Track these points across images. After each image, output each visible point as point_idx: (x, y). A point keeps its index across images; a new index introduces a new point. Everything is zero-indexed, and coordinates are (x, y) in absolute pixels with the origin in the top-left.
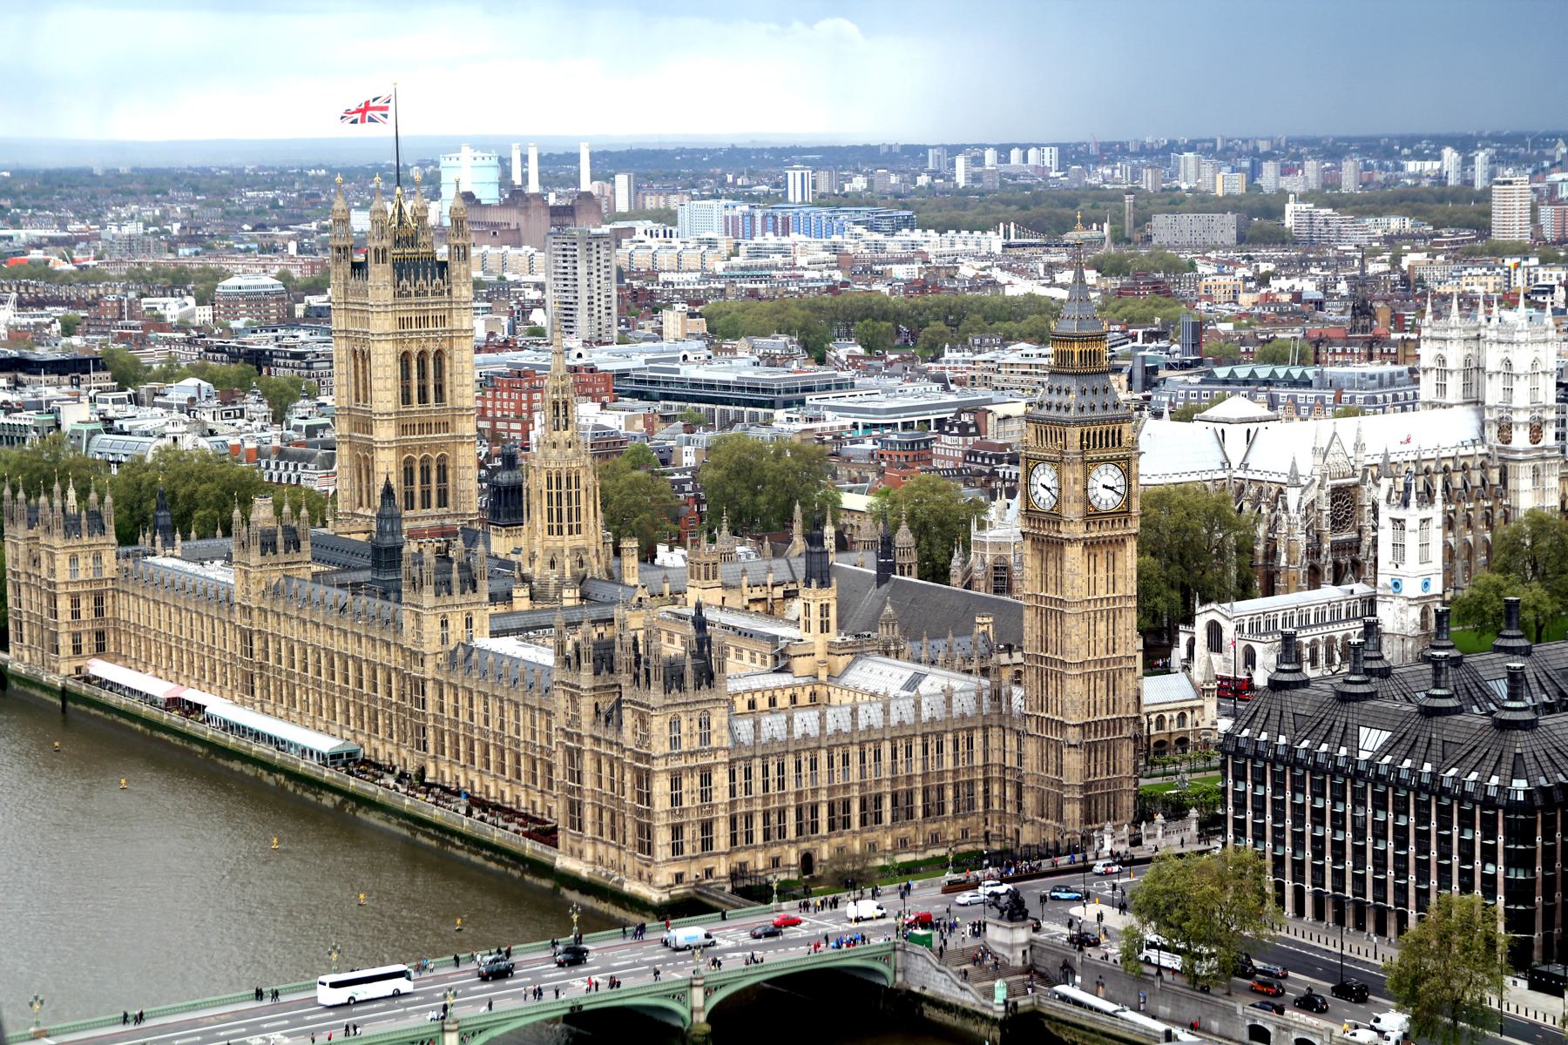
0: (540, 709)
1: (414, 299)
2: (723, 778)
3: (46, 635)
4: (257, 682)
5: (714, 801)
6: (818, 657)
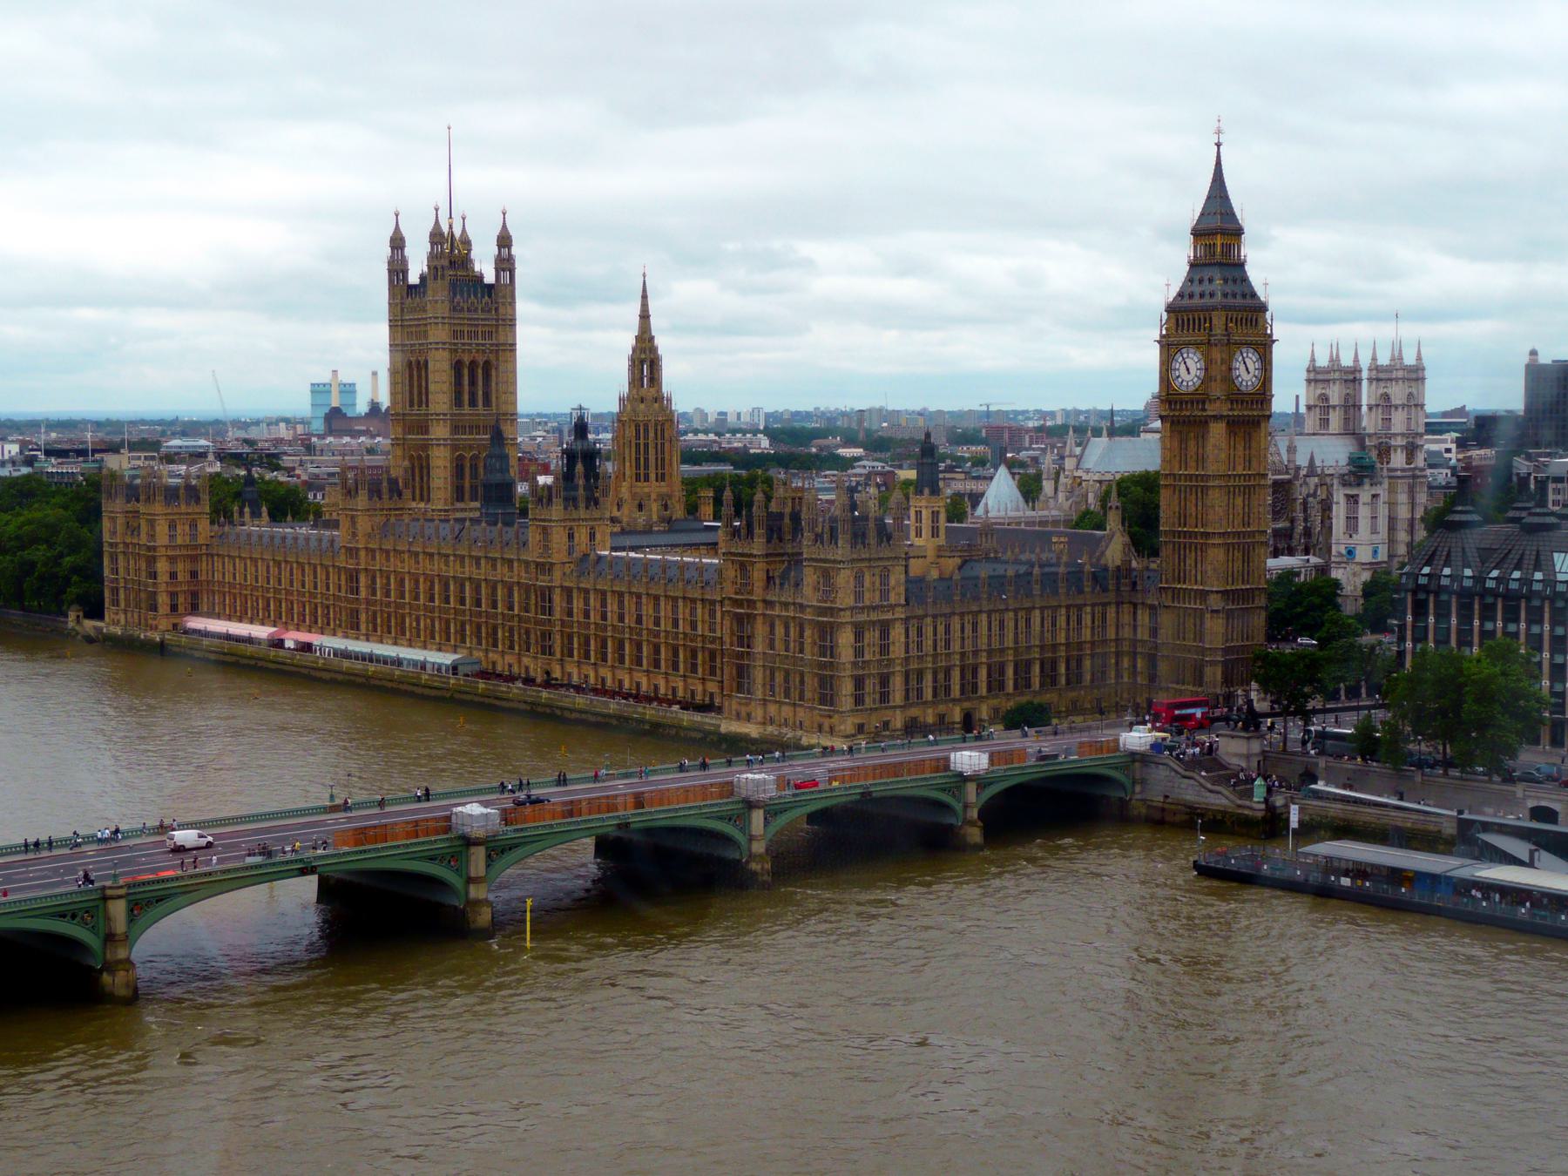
0: (684, 598)
1: (466, 315)
2: (900, 634)
3: (143, 595)
4: (363, 617)
5: (892, 656)
6: (929, 559)
